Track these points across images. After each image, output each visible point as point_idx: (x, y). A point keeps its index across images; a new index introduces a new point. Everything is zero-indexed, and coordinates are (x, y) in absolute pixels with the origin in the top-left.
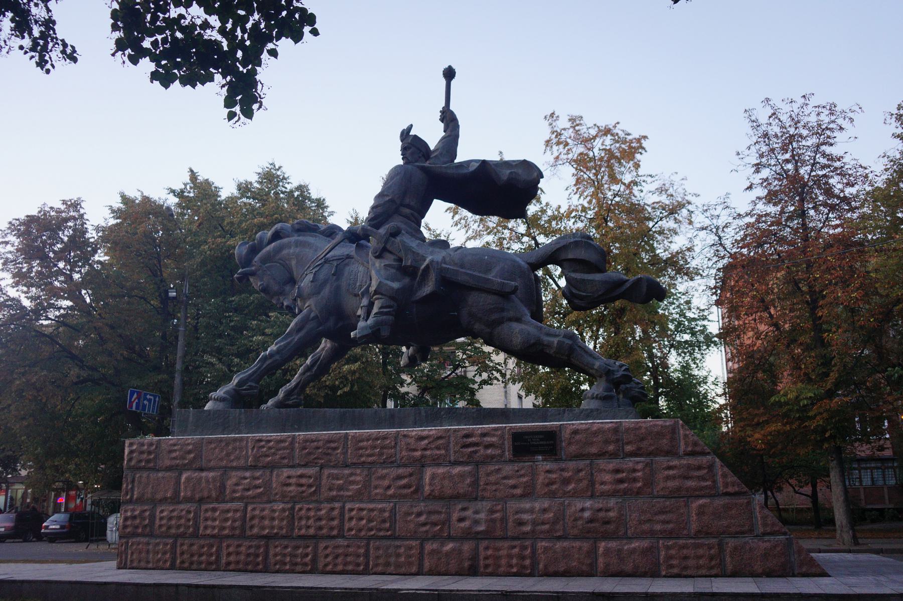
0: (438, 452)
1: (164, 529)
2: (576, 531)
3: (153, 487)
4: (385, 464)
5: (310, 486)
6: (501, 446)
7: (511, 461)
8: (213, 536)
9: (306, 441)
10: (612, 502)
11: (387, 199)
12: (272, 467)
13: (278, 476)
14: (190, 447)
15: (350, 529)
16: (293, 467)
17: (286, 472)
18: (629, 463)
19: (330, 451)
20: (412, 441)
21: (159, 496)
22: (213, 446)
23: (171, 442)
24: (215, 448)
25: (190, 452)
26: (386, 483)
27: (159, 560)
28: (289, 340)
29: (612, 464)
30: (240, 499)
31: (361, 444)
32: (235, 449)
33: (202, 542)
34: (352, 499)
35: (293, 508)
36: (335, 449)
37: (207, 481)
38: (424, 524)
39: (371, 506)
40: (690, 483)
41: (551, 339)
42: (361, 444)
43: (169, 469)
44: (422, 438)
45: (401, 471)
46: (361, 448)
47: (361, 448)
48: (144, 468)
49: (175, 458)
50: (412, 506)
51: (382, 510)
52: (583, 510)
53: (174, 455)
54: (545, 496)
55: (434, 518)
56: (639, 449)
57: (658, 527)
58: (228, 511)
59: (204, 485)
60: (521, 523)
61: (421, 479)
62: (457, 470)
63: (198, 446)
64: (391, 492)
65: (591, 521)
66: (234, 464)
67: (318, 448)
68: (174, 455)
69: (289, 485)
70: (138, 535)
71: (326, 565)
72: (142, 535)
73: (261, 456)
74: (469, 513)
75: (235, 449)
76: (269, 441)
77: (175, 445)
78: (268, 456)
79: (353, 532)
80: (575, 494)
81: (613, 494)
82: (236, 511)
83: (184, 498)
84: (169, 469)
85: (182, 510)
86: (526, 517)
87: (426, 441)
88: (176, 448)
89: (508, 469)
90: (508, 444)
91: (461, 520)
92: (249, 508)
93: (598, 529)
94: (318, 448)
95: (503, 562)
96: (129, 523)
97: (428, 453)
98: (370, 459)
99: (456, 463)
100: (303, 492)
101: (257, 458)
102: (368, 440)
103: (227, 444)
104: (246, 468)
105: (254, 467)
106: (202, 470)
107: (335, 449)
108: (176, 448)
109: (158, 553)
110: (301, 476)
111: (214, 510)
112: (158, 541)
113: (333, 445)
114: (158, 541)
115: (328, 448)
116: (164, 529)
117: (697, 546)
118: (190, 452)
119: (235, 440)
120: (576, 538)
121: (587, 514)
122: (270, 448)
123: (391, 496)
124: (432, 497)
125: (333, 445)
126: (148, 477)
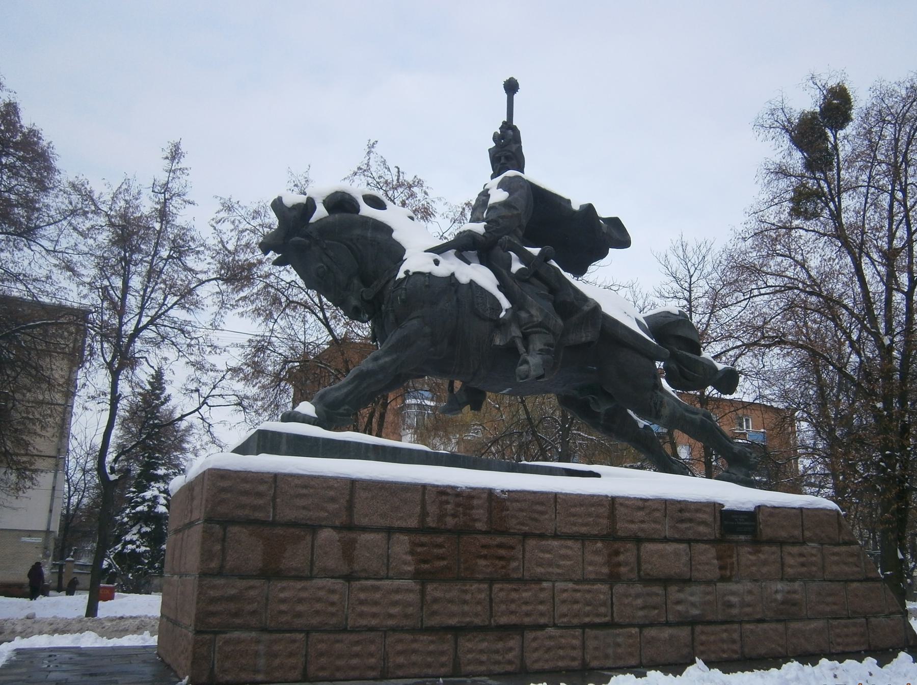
0: (653, 525)
11: (515, 212)
19: (536, 516)
29: (795, 550)
31: (573, 510)
36: (542, 513)
40: (846, 569)
41: (693, 416)
42: (573, 510)
52: (777, 592)
60: (730, 605)
65: (783, 603)
86: (734, 599)
94: (521, 510)
102: (581, 505)
113: (539, 508)
121: (779, 597)
125: (539, 508)
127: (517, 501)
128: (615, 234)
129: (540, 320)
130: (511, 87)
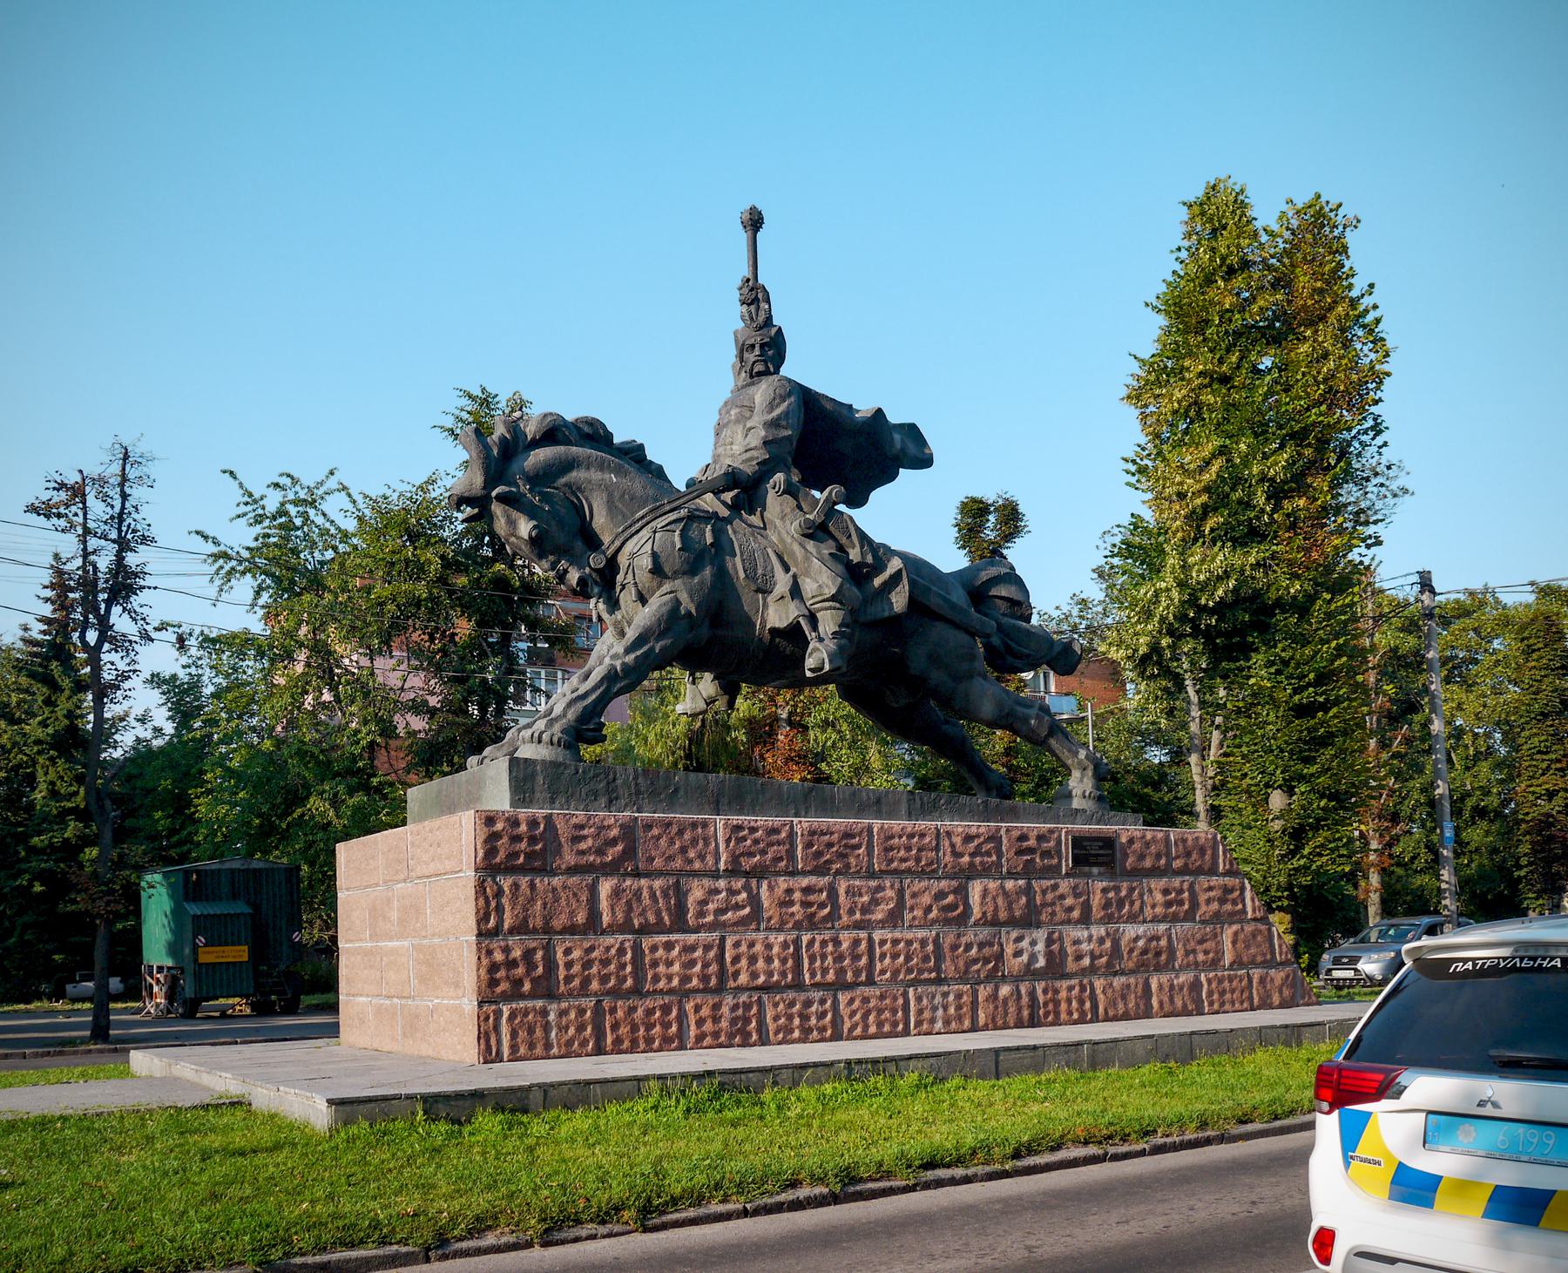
1: (576, 982)
2: (1131, 965)
3: (545, 904)
4: (922, 874)
5: (822, 906)
6: (1059, 853)
7: (1068, 875)
8: (671, 992)
9: (812, 833)
10: (1162, 927)
12: (760, 873)
13: (771, 888)
14: (614, 832)
15: (883, 972)
16: (793, 873)
17: (783, 883)
18: (1176, 882)
20: (958, 840)
21: (557, 923)
22: (655, 831)
23: (574, 820)
24: (659, 838)
25: (614, 842)
26: (926, 899)
27: (569, 1043)
28: (645, 648)
30: (712, 927)
32: (694, 841)
33: (649, 1003)
34: (882, 924)
35: (797, 942)
37: (653, 896)
38: (975, 961)
39: (909, 935)
43: (573, 870)
44: (968, 838)
45: (944, 884)
46: (892, 849)
47: (892, 849)
48: (522, 870)
49: (583, 853)
50: (959, 936)
51: (923, 943)
53: (583, 846)
54: (1101, 921)
55: (986, 951)
56: (1186, 865)
57: (1201, 957)
58: (693, 948)
59: (646, 901)
61: (967, 897)
62: (1009, 884)
63: (628, 830)
64: (933, 915)
66: (697, 865)
67: (830, 845)
68: (583, 846)
69: (792, 903)
70: (523, 997)
71: (854, 1027)
72: (533, 995)
73: (742, 854)
74: (1025, 944)
75: (694, 841)
76: (753, 830)
77: (582, 827)
78: (752, 855)
79: (888, 975)
80: (1133, 918)
81: (1164, 919)
82: (707, 948)
83: (609, 926)
84: (573, 870)
85: (608, 949)
86: (1085, 947)
87: (976, 842)
88: (585, 832)
89: (1065, 886)
90: (1067, 851)
91: (1018, 954)
92: (729, 943)
93: (1155, 959)
94: (830, 845)
95: (1064, 1006)
96: (501, 974)
97: (978, 860)
98: (904, 866)
99: (1012, 875)
100: (813, 915)
101: (735, 859)
102: (900, 837)
103: (681, 832)
104: (715, 875)
105: (733, 872)
106: (637, 874)
107: (858, 846)
108: (585, 832)
109: (567, 1028)
110: (807, 890)
111: (669, 946)
112: (564, 1005)
114: (564, 1005)
115: (846, 846)
116: (576, 982)
117: (1231, 980)
118: (614, 842)
119: (694, 825)
120: (1132, 972)
121: (1141, 943)
122: (756, 842)
123: (934, 922)
124: (984, 921)
126: (532, 886)
127: (823, 834)
128: (912, 449)
129: (834, 591)
130: (754, 222)
